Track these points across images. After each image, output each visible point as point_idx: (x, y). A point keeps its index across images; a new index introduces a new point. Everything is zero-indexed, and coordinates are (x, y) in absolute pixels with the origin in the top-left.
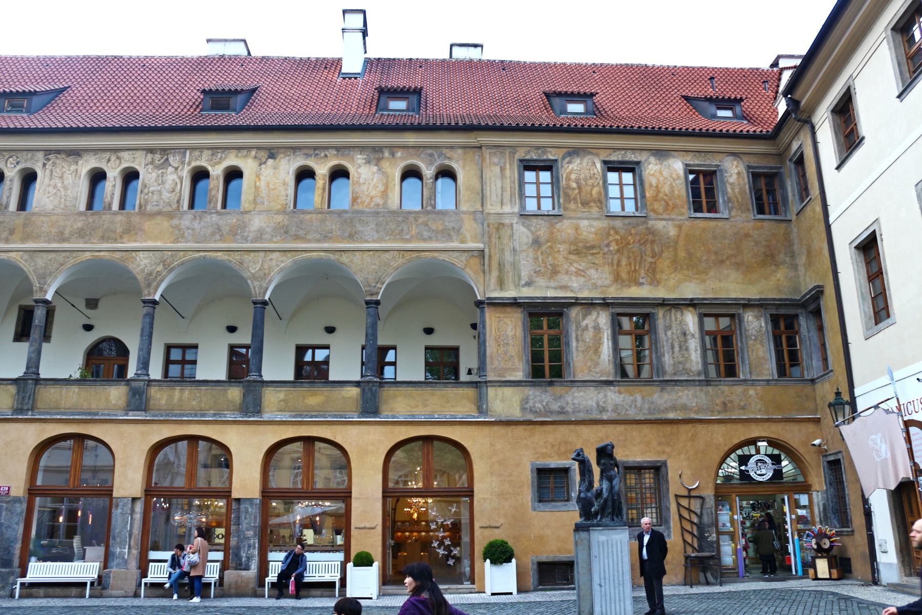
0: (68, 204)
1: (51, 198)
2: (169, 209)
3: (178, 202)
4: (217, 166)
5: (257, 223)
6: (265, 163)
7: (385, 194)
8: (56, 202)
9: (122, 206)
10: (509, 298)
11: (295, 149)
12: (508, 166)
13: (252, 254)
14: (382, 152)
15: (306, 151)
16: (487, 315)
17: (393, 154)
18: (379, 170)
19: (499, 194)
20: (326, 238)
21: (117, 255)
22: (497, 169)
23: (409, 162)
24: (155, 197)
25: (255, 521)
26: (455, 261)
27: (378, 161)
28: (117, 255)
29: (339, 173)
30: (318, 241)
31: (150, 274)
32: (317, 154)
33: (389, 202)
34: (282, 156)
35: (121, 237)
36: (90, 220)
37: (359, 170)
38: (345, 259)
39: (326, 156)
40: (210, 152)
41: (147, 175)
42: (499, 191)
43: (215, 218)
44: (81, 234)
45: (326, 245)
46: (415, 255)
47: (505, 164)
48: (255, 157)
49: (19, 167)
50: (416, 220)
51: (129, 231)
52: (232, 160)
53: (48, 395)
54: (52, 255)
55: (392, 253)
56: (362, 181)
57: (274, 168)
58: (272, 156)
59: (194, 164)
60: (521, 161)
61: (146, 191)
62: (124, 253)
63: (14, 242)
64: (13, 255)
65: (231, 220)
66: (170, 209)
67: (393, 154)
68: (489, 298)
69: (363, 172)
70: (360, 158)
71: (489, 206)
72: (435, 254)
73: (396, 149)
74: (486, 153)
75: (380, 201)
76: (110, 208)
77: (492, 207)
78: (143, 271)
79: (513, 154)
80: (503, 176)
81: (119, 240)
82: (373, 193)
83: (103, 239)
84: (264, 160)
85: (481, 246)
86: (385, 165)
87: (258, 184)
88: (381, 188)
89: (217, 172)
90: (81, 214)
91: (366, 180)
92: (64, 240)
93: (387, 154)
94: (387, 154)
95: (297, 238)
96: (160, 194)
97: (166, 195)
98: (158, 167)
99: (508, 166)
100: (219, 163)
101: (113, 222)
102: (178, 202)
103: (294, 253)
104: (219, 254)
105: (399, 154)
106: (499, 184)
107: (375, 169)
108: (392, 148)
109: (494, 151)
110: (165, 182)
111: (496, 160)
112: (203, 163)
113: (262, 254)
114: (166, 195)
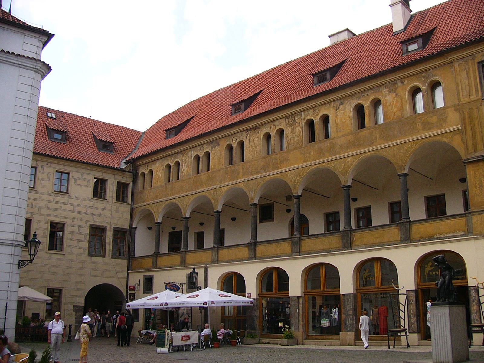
0: (258, 154)
1: (251, 153)
2: (298, 146)
3: (302, 141)
4: (317, 117)
5: (340, 142)
6: (339, 108)
7: (401, 108)
8: (253, 155)
9: (281, 149)
10: (479, 157)
11: (352, 96)
12: (471, 69)
13: (339, 161)
14: (397, 84)
15: (357, 96)
16: (468, 170)
17: (402, 83)
18: (397, 95)
19: (467, 90)
20: (372, 143)
21: (279, 176)
22: (464, 74)
23: (412, 85)
24: (292, 141)
25: (352, 307)
26: (446, 140)
27: (395, 89)
28: (279, 176)
29: (377, 103)
30: (370, 146)
31: (295, 182)
32: (363, 95)
33: (404, 113)
34: (347, 101)
35: (281, 166)
36: (267, 160)
37: (386, 98)
38: (384, 153)
39: (368, 95)
40: (313, 110)
41: (288, 132)
42: (467, 87)
43: (320, 145)
44: (265, 168)
45: (373, 148)
46: (423, 141)
47: (469, 69)
48: (334, 107)
49: (237, 141)
50: (421, 120)
51: (284, 161)
52: (323, 111)
53: (260, 249)
54: (254, 181)
55: (409, 143)
56: (388, 104)
57: (344, 110)
58: (341, 104)
59: (306, 119)
60: (479, 63)
61: (288, 139)
62: (282, 174)
63: (240, 178)
64: (239, 184)
65: (327, 143)
66: (299, 146)
67: (402, 83)
68: (465, 160)
69: (388, 97)
70: (385, 91)
71: (462, 100)
72: (433, 138)
73: (404, 80)
74: (456, 65)
75: (399, 113)
76: (274, 152)
77: (464, 100)
78: (291, 181)
79: (473, 59)
80: (468, 77)
81: (280, 167)
82: (395, 110)
83: (274, 168)
84: (338, 107)
85: (459, 126)
86: (399, 90)
87: (337, 121)
88: (399, 105)
89: (317, 119)
90: (264, 158)
91: (390, 103)
92: (258, 173)
93: (399, 84)
94: (399, 84)
95: (359, 146)
96: (294, 139)
97: (296, 138)
98: (291, 125)
99: (471, 69)
100: (318, 115)
101: (276, 159)
102: (302, 141)
103: (358, 155)
104: (324, 164)
105: (406, 82)
106: (467, 83)
107: (394, 95)
108: (402, 80)
109: (461, 62)
110: (296, 132)
111: (463, 67)
112: (310, 117)
113: (343, 160)
114: (296, 138)
